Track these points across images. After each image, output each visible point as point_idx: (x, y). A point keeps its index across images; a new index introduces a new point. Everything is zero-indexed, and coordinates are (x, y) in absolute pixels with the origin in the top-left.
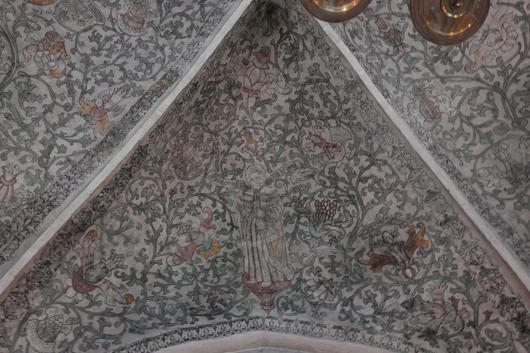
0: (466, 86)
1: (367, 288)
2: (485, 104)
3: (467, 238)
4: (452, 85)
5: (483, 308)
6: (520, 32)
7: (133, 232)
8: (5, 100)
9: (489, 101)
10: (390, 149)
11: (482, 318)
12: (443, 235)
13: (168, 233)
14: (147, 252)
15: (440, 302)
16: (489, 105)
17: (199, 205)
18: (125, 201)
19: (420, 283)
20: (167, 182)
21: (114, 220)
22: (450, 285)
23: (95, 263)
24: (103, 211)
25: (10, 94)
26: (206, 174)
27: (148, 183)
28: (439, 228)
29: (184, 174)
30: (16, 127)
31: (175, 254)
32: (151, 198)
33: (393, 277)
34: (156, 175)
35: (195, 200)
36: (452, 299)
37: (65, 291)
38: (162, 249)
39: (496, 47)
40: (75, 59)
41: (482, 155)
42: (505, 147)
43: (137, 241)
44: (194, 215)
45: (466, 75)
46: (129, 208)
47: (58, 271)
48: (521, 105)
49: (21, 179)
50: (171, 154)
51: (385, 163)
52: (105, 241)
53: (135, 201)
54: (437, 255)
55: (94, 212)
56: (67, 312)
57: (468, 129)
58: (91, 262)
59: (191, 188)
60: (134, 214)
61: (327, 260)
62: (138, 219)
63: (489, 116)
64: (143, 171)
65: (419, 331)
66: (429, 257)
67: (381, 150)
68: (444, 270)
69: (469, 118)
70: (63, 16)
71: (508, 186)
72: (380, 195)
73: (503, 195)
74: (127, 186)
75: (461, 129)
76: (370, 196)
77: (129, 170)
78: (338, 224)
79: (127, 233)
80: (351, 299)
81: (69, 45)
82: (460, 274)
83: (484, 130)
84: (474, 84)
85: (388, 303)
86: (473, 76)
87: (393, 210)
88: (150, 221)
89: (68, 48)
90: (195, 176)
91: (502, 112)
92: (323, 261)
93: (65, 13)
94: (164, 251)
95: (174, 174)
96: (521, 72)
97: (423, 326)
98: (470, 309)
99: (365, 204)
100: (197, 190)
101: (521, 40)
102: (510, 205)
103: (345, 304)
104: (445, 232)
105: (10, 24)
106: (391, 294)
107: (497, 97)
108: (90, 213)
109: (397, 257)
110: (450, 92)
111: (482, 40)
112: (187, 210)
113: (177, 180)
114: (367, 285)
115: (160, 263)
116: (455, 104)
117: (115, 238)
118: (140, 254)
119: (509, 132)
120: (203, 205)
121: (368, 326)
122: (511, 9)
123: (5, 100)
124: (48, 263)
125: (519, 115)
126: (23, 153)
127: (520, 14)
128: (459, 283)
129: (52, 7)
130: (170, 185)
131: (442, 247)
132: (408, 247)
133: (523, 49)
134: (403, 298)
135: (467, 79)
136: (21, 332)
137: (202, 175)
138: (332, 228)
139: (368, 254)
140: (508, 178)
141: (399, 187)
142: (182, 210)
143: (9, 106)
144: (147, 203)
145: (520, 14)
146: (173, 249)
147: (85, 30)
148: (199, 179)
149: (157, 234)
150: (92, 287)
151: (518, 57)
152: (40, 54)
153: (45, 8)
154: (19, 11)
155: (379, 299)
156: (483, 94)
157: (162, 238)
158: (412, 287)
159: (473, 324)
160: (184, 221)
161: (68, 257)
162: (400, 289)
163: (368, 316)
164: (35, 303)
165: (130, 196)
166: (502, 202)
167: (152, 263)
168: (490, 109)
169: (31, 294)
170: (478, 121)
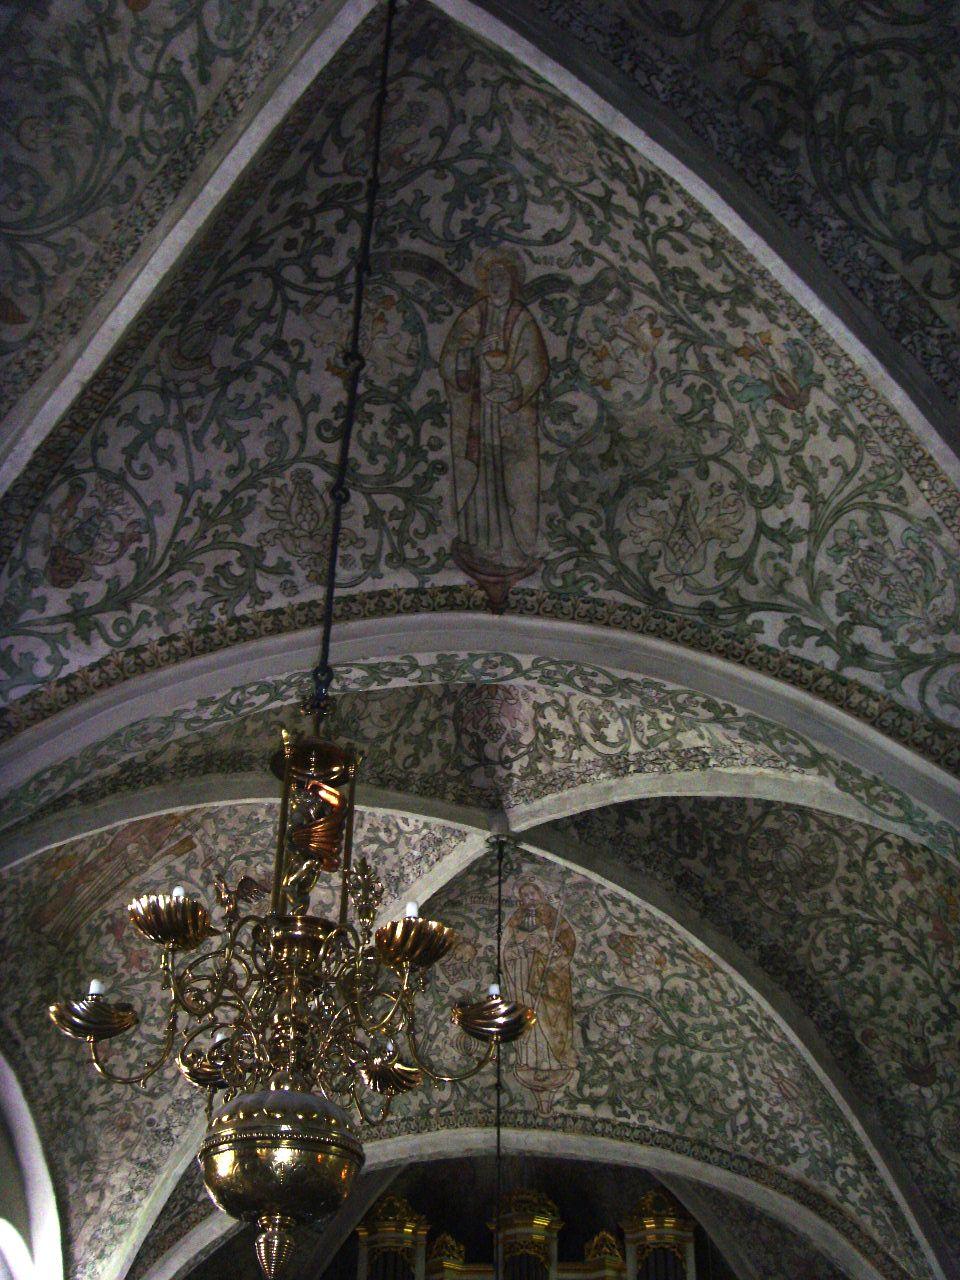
7: (885, 981)
8: (687, 1030)
13: (906, 934)
14: (921, 978)
17: (881, 865)
18: (836, 982)
20: (830, 906)
21: (858, 1003)
23: (906, 1046)
24: (841, 1017)
25: (680, 1020)
26: (837, 833)
27: (820, 942)
29: (824, 870)
30: (720, 1036)
31: (939, 947)
32: (847, 941)
34: (812, 928)
35: (871, 868)
37: (922, 1097)
38: (926, 958)
40: (642, 932)
43: (901, 981)
44: (894, 881)
46: (850, 976)
47: (896, 1092)
49: (779, 1067)
50: (786, 898)
52: (883, 1021)
53: (841, 967)
55: (838, 1029)
56: (945, 1111)
58: (903, 1050)
59: (852, 866)
60: (860, 970)
62: (869, 967)
64: (799, 951)
70: (587, 921)
74: (814, 977)
77: (791, 975)
79: (883, 988)
81: (622, 929)
88: (879, 950)
89: (627, 932)
90: (835, 851)
93: (582, 918)
94: (930, 956)
95: (818, 891)
100: (858, 858)
105: (600, 986)
108: (836, 1035)
112: (883, 888)
113: (831, 887)
115: (942, 974)
117: (885, 1007)
118: (919, 987)
120: (884, 859)
123: (687, 1030)
124: (880, 1100)
126: (750, 1046)
129: (577, 931)
130: (836, 901)
136: (944, 1162)
137: (836, 838)
142: (881, 896)
143: (694, 1029)
144: (850, 948)
146: (931, 943)
147: (605, 906)
148: (842, 848)
149: (901, 948)
150: (932, 1068)
152: (635, 965)
153: (579, 939)
154: (584, 971)
157: (911, 948)
160: (898, 901)
161: (883, 1074)
164: (919, 1130)
165: (832, 973)
167: (937, 982)
169: (908, 1130)
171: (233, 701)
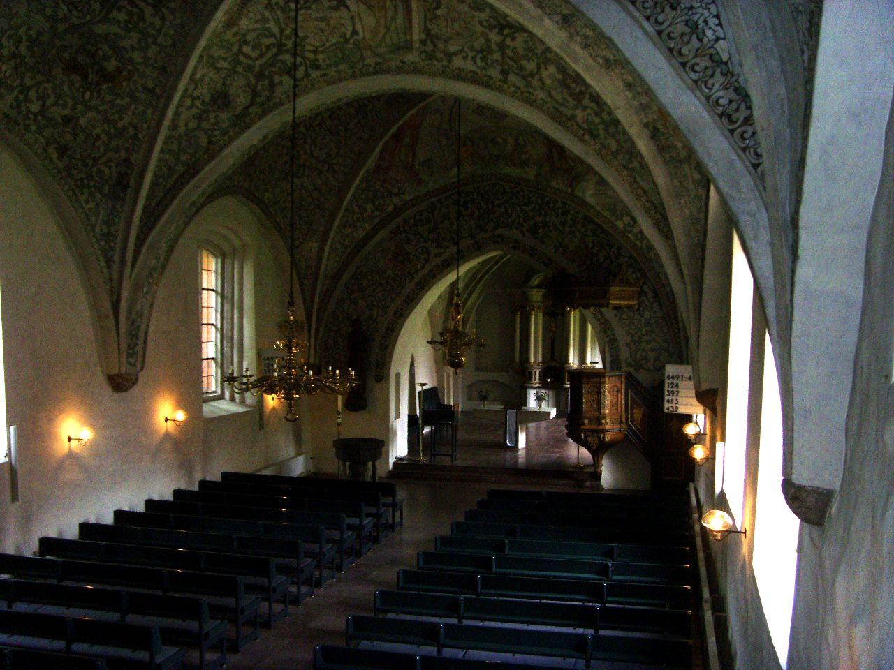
0: (273, 26)
1: (47, 85)
2: (263, 47)
3: (149, 112)
4: (267, 14)
5: (109, 155)
6: (334, 41)
9: (268, 47)
10: (178, 21)
11: (103, 160)
12: (138, 94)
15: (88, 131)
16: (264, 50)
19: (88, 108)
22: (105, 126)
28: (141, 88)
33: (73, 90)
36: (98, 137)
39: (316, 31)
41: (218, 70)
42: (236, 78)
45: (281, 21)
48: (275, 69)
51: (163, 19)
54: (118, 101)
57: (235, 48)
61: (33, 33)
63: (254, 54)
65: (58, 143)
66: (112, 97)
67: (173, 12)
68: (113, 114)
69: (246, 43)
71: (207, 99)
72: (130, 26)
73: (198, 103)
75: (232, 44)
76: (122, 17)
78: (70, 7)
80: (29, 89)
82: (120, 125)
83: (242, 58)
84: (276, 30)
85: (53, 109)
86: (283, 26)
87: (126, 43)
91: (262, 61)
92: (31, 32)
96: (302, 56)
97: (63, 141)
98: (102, 149)
99: (111, 16)
101: (328, 44)
102: (194, 111)
103: (21, 92)
104: (141, 95)
106: (61, 102)
107: (274, 50)
109: (90, 76)
110: (260, 17)
111: (317, 19)
114: (49, 81)
116: (250, 27)
119: (250, 75)
121: (28, 122)
122: (350, 28)
125: (266, 73)
127: (348, 36)
128: (112, 130)
131: (127, 100)
132: (106, 77)
133: (321, 49)
134: (65, 112)
135: (278, 23)
138: (64, 7)
139: (71, 54)
140: (213, 97)
141: (150, 40)
145: (348, 35)
151: (314, 48)
155: (49, 102)
156: (272, 40)
158: (80, 108)
159: (95, 160)
162: (71, 103)
163: (32, 113)
166: (193, 106)
168: (261, 52)
170: (246, 49)
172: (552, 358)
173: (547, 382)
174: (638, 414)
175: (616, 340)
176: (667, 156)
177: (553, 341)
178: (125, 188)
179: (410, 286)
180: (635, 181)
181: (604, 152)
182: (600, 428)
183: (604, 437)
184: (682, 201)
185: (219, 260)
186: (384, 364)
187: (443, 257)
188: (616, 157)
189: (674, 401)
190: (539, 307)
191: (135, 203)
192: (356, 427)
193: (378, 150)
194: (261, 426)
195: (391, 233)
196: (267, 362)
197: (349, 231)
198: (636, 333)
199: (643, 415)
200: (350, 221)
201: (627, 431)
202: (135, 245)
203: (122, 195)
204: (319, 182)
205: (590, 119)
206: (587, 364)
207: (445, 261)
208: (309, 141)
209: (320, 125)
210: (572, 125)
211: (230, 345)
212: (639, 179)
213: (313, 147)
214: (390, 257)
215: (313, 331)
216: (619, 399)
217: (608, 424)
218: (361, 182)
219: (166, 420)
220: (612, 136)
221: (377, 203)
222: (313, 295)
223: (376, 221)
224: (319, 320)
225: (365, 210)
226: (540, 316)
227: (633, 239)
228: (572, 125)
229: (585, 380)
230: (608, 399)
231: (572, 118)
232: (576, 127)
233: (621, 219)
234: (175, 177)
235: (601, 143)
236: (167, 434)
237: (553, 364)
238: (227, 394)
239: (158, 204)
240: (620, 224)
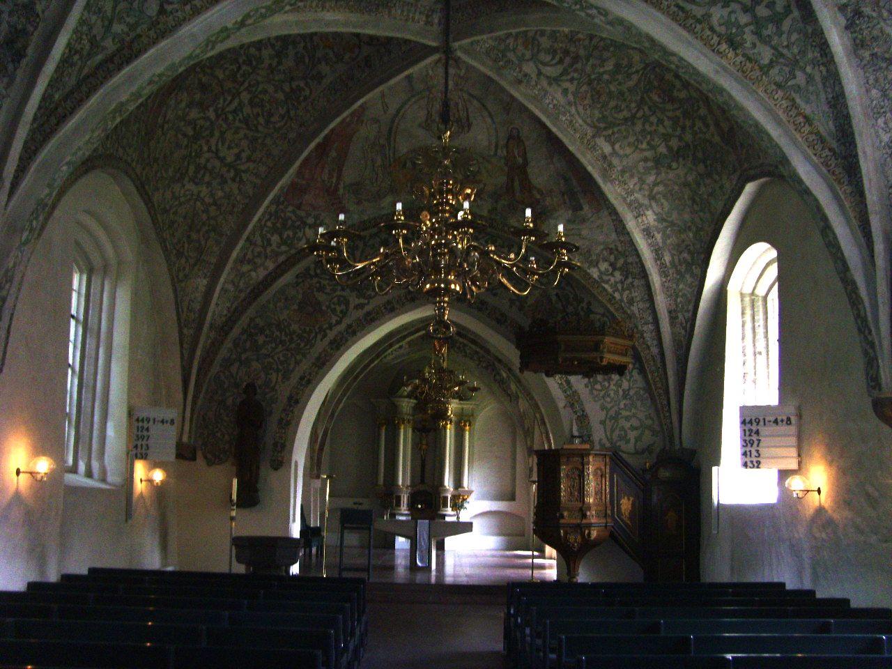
171: (578, 7)
172: (422, 481)
173: (418, 508)
174: (626, 504)
175: (586, 416)
176: (867, 54)
177: (423, 466)
178: (19, 56)
179: (320, 345)
180: (794, 105)
181: (749, 65)
182: (584, 521)
183: (589, 534)
184: (881, 121)
185: (85, 277)
186: (283, 446)
187: (367, 308)
188: (766, 74)
189: (754, 453)
190: (409, 422)
191: (31, 85)
192: (252, 525)
193: (298, 163)
194: (129, 514)
195: (297, 277)
196: (140, 424)
197: (245, 268)
198: (613, 407)
199: (633, 505)
200: (249, 256)
201: (613, 527)
202: (21, 159)
203: (10, 67)
204: (220, 194)
205: (733, 20)
206: (463, 487)
207: (368, 314)
208: (217, 134)
209: (235, 112)
210: (703, 30)
211: (90, 396)
212: (798, 101)
213: (220, 144)
214: (296, 307)
215: (190, 397)
216: (604, 487)
217: (593, 517)
218: (272, 203)
219: (18, 472)
220: (766, 41)
221: (285, 236)
222: (193, 351)
223: (282, 259)
224: (198, 385)
225: (269, 243)
226: (410, 431)
227: (610, 290)
228: (703, 30)
229: (563, 460)
230: (591, 485)
231: (707, 16)
232: (709, 33)
233: (596, 265)
234: (100, 57)
235: (744, 55)
236: (17, 494)
237: (422, 488)
238: (82, 467)
239: (65, 98)
240: (594, 273)
